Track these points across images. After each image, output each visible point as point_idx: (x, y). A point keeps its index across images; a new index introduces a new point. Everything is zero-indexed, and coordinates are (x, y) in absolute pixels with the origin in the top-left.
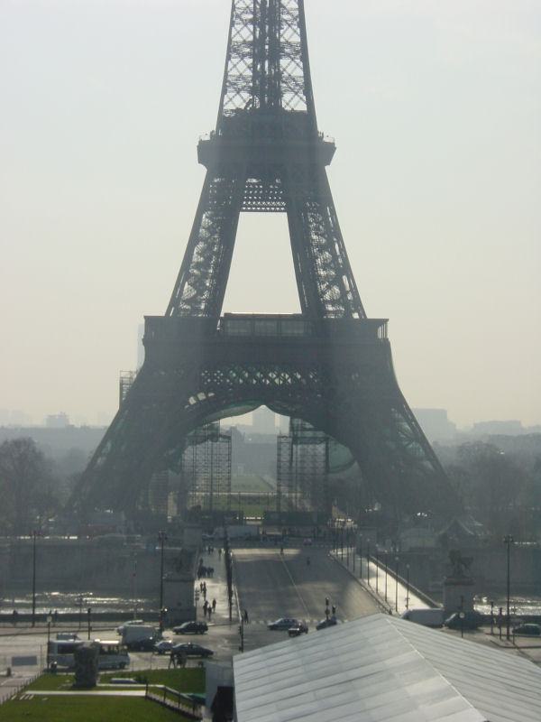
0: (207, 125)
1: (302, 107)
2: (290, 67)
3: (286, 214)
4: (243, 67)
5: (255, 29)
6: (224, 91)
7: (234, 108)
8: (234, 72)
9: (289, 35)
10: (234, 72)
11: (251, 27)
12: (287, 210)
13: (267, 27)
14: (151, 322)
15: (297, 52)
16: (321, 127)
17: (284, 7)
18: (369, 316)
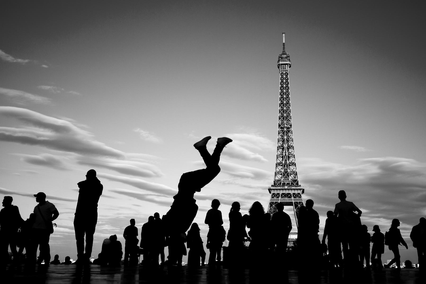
6: (276, 175)
8: (278, 170)
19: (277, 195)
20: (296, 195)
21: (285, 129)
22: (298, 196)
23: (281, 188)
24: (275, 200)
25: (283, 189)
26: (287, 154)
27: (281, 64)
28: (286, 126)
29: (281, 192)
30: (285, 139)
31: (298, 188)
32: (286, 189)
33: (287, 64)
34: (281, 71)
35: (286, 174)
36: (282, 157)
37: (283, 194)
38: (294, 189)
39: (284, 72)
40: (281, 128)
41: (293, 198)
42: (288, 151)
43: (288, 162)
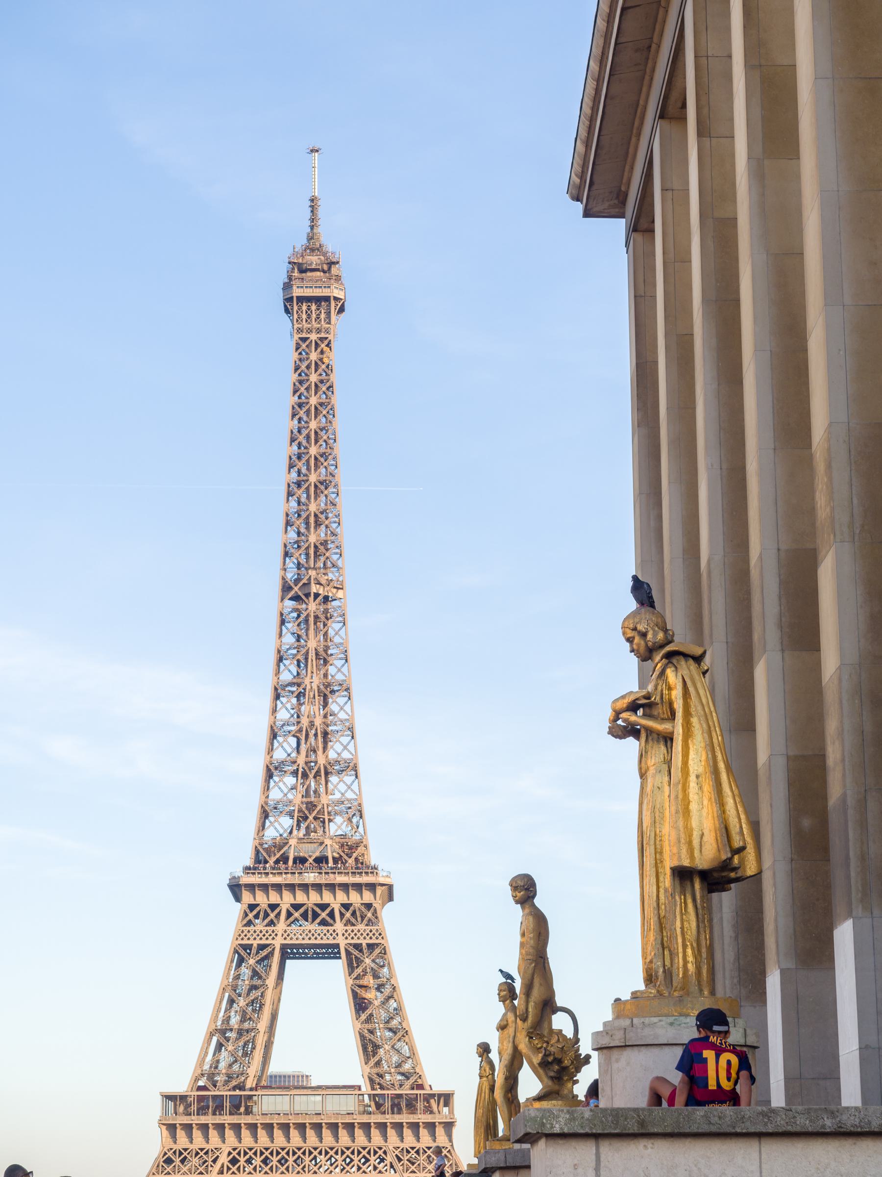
2: (340, 786)
4: (285, 787)
9: (336, 750)
10: (275, 794)
11: (293, 741)
12: (340, 958)
14: (169, 1098)
16: (374, 857)
19: (266, 915)
20: (354, 914)
23: (290, 879)
25: (291, 887)
26: (318, 721)
27: (301, 299)
28: (314, 589)
29: (287, 900)
30: (312, 655)
32: (305, 887)
33: (327, 299)
34: (300, 330)
37: (297, 907)
38: (345, 887)
39: (313, 337)
40: (296, 598)
41: (339, 926)
43: (322, 761)
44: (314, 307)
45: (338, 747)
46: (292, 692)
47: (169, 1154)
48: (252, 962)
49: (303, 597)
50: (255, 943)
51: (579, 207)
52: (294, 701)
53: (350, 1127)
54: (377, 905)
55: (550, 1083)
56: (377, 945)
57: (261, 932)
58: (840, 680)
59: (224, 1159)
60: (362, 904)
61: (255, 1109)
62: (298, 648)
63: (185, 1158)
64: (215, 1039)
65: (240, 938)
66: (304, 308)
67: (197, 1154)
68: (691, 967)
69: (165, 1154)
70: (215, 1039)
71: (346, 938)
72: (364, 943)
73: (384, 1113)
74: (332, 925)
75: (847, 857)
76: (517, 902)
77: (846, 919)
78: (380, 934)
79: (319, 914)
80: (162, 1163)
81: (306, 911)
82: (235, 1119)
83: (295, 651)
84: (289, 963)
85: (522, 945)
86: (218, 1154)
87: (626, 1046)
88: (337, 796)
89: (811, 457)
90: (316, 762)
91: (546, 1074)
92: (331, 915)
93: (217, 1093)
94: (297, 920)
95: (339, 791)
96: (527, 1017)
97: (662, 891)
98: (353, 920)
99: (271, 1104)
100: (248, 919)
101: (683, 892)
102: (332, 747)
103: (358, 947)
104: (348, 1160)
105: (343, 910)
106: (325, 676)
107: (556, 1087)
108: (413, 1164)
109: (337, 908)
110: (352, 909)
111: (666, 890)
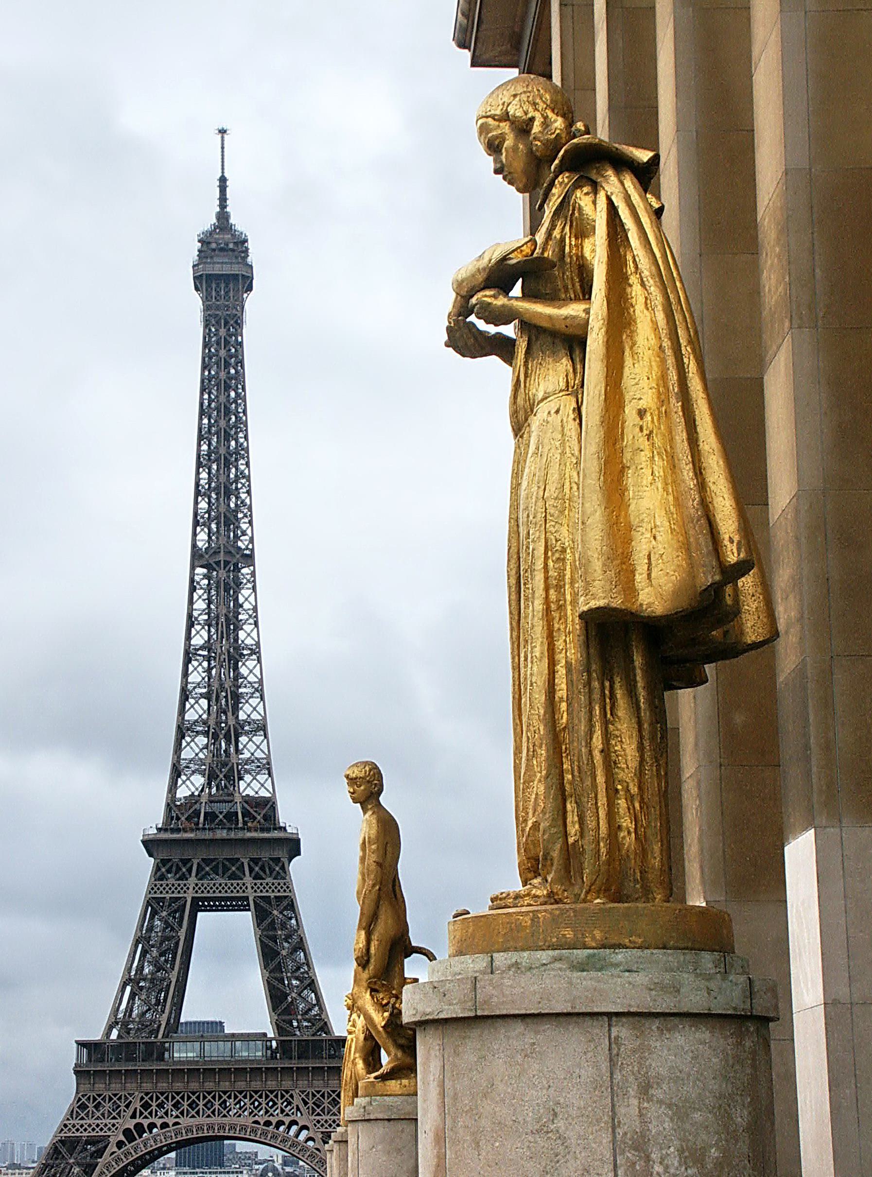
0: (153, 817)
1: (264, 793)
2: (250, 747)
3: (249, 913)
4: (196, 747)
5: (209, 706)
7: (189, 793)
10: (187, 754)
11: (204, 702)
12: (249, 910)
13: (223, 702)
15: (258, 729)
17: (246, 678)
18: (336, 1034)
19: (179, 869)
20: (262, 868)
21: (223, 574)
22: (272, 871)
24: (171, 889)
27: (209, 276)
31: (276, 834)
35: (223, 771)
36: (207, 696)
42: (236, 668)
43: (231, 722)
44: (223, 286)
45: (247, 708)
46: (203, 656)
47: (83, 1100)
48: (164, 914)
49: (214, 565)
50: (168, 896)
51: (467, 54)
52: (205, 664)
53: (256, 1072)
54: (286, 861)
55: (399, 1054)
56: (286, 897)
57: (173, 885)
58: (797, 511)
59: (137, 1105)
60: (270, 858)
61: (166, 1055)
62: (209, 614)
63: (99, 1103)
64: (128, 989)
65: (152, 892)
66: (214, 286)
67: (110, 1099)
68: (628, 841)
69: (80, 1099)
70: (128, 989)
71: (255, 891)
72: (272, 895)
73: (291, 1058)
74: (242, 879)
75: (807, 747)
76: (355, 801)
77: (806, 829)
78: (288, 887)
79: (229, 869)
80: (76, 1109)
81: (217, 866)
82: (147, 1066)
83: (206, 617)
84: (200, 914)
85: (363, 859)
86: (131, 1099)
87: (477, 1017)
88: (246, 755)
89: (752, 226)
90: (226, 723)
91: (395, 1042)
92: (241, 868)
93: (131, 1040)
94: (208, 874)
95: (249, 751)
96: (368, 961)
97: (561, 670)
98: (261, 873)
99: (183, 1053)
100: (159, 874)
101: (607, 674)
102: (241, 708)
103: (267, 899)
104: (256, 1104)
105: (251, 863)
106: (236, 639)
107: (408, 1060)
108: (318, 1107)
109: (246, 862)
110: (260, 863)
111: (568, 666)
